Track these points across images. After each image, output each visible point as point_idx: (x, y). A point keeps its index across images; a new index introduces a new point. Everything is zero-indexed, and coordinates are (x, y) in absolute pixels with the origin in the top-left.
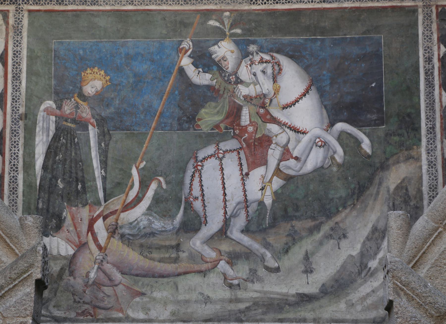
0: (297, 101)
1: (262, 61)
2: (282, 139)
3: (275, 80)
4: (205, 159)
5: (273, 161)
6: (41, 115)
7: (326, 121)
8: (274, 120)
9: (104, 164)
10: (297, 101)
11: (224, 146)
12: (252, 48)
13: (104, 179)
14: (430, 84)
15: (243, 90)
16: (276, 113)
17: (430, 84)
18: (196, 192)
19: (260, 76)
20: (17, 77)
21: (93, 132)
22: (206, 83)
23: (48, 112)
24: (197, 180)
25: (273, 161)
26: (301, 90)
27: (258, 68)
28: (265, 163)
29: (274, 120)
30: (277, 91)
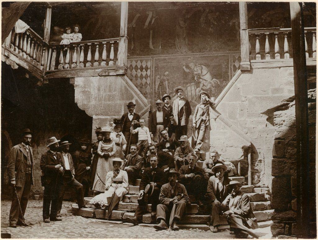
0: (206, 74)
1: (199, 67)
2: (203, 82)
3: (201, 70)
4: (188, 87)
5: (201, 87)
6: (157, 79)
7: (211, 79)
8: (201, 78)
9: (168, 88)
10: (206, 74)
11: (192, 84)
12: (197, 64)
13: (169, 91)
14: (231, 71)
15: (195, 73)
16: (201, 77)
17: (231, 71)
18: (186, 93)
19: (198, 69)
20: (152, 72)
21: (167, 82)
22: (188, 71)
23: (159, 78)
24: (186, 91)
25: (201, 87)
26: (207, 72)
27: (198, 68)
28: (199, 87)
29: (201, 78)
30: (202, 73)
